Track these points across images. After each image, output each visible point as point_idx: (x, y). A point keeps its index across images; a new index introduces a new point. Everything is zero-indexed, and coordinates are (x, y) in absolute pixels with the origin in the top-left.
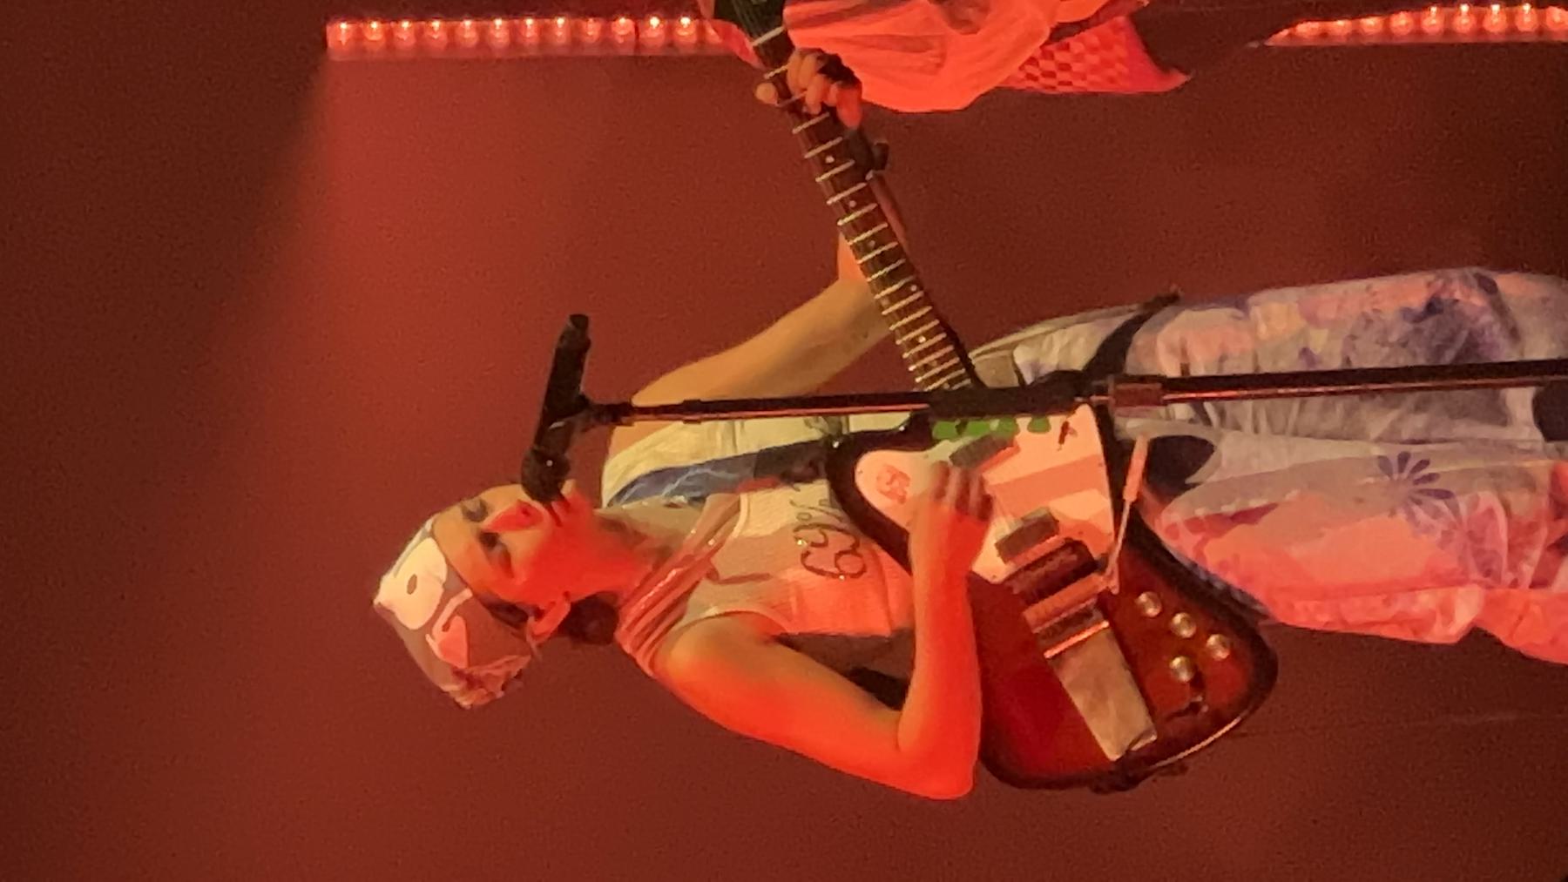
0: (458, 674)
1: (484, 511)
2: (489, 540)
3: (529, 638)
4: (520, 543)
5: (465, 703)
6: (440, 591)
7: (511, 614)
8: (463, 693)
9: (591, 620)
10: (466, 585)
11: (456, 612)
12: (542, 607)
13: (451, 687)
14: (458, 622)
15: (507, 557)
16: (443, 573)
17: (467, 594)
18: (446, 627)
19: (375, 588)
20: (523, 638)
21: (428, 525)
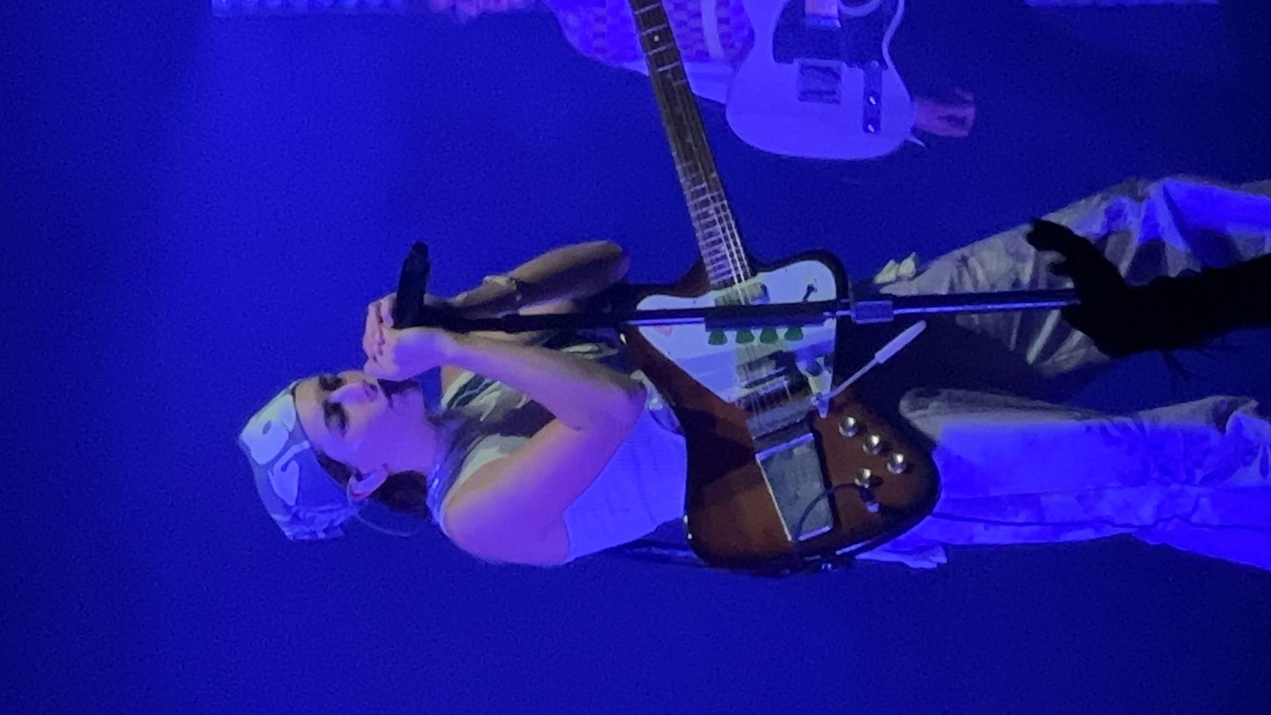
10: (307, 438)
11: (296, 457)
14: (294, 466)
17: (306, 445)
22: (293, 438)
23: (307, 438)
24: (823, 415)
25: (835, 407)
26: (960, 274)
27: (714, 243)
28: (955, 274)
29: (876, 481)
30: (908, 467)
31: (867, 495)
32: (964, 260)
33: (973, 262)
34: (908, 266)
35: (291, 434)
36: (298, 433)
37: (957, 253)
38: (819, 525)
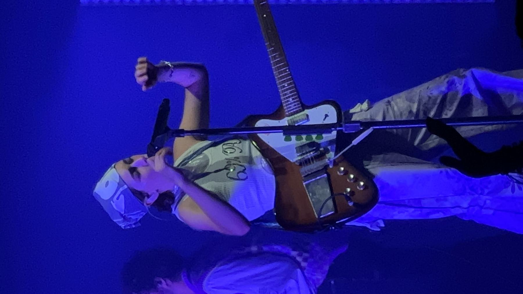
0: (122, 215)
1: (132, 161)
2: (133, 170)
3: (145, 204)
5: (122, 225)
7: (140, 195)
8: (123, 221)
10: (125, 184)
11: (122, 193)
12: (149, 194)
13: (118, 220)
14: (122, 196)
15: (139, 175)
16: (118, 181)
17: (126, 187)
18: (118, 199)
19: (95, 185)
20: (143, 205)
21: (113, 165)
22: (120, 185)
23: (125, 184)
24: (331, 167)
25: (336, 163)
26: (388, 109)
27: (287, 98)
28: (386, 107)
29: (352, 193)
31: (348, 198)
32: (389, 102)
33: (392, 103)
34: (365, 105)
35: (118, 184)
36: (122, 182)
37: (386, 100)
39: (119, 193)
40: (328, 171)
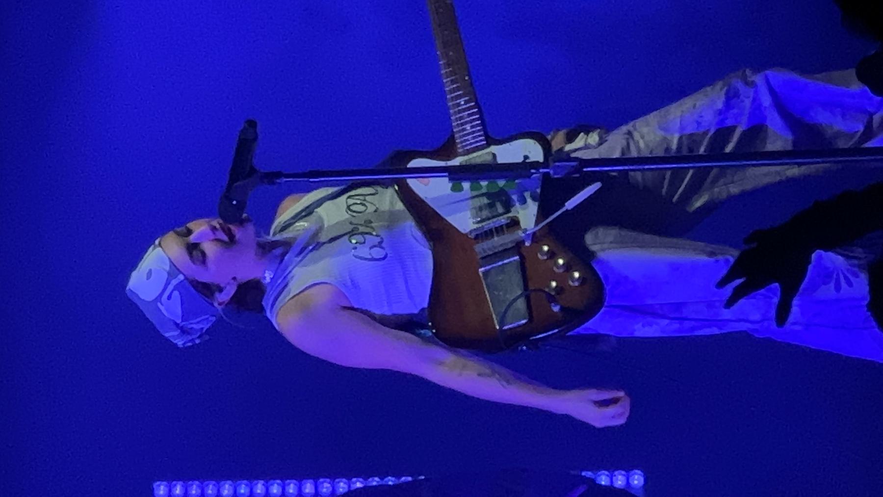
2: (193, 248)
4: (209, 248)
6: (166, 276)
7: (207, 290)
8: (178, 337)
9: (251, 296)
10: (181, 272)
14: (176, 293)
15: (203, 254)
16: (167, 268)
17: (181, 277)
23: (181, 272)
28: (624, 143)
30: (582, 280)
32: (629, 133)
33: (636, 135)
36: (174, 270)
37: (624, 129)
38: (518, 320)
39: (170, 287)
40: (523, 251)
